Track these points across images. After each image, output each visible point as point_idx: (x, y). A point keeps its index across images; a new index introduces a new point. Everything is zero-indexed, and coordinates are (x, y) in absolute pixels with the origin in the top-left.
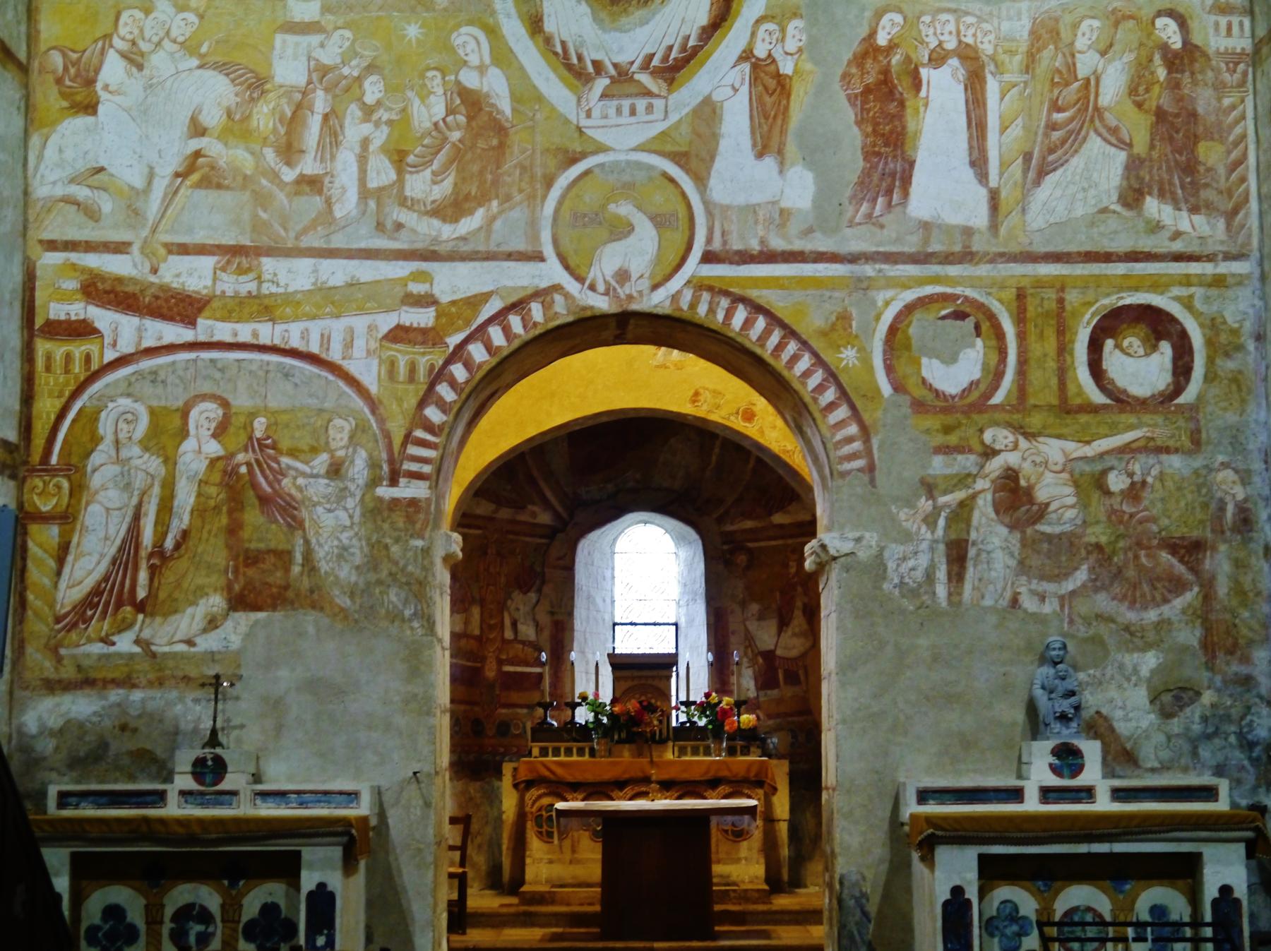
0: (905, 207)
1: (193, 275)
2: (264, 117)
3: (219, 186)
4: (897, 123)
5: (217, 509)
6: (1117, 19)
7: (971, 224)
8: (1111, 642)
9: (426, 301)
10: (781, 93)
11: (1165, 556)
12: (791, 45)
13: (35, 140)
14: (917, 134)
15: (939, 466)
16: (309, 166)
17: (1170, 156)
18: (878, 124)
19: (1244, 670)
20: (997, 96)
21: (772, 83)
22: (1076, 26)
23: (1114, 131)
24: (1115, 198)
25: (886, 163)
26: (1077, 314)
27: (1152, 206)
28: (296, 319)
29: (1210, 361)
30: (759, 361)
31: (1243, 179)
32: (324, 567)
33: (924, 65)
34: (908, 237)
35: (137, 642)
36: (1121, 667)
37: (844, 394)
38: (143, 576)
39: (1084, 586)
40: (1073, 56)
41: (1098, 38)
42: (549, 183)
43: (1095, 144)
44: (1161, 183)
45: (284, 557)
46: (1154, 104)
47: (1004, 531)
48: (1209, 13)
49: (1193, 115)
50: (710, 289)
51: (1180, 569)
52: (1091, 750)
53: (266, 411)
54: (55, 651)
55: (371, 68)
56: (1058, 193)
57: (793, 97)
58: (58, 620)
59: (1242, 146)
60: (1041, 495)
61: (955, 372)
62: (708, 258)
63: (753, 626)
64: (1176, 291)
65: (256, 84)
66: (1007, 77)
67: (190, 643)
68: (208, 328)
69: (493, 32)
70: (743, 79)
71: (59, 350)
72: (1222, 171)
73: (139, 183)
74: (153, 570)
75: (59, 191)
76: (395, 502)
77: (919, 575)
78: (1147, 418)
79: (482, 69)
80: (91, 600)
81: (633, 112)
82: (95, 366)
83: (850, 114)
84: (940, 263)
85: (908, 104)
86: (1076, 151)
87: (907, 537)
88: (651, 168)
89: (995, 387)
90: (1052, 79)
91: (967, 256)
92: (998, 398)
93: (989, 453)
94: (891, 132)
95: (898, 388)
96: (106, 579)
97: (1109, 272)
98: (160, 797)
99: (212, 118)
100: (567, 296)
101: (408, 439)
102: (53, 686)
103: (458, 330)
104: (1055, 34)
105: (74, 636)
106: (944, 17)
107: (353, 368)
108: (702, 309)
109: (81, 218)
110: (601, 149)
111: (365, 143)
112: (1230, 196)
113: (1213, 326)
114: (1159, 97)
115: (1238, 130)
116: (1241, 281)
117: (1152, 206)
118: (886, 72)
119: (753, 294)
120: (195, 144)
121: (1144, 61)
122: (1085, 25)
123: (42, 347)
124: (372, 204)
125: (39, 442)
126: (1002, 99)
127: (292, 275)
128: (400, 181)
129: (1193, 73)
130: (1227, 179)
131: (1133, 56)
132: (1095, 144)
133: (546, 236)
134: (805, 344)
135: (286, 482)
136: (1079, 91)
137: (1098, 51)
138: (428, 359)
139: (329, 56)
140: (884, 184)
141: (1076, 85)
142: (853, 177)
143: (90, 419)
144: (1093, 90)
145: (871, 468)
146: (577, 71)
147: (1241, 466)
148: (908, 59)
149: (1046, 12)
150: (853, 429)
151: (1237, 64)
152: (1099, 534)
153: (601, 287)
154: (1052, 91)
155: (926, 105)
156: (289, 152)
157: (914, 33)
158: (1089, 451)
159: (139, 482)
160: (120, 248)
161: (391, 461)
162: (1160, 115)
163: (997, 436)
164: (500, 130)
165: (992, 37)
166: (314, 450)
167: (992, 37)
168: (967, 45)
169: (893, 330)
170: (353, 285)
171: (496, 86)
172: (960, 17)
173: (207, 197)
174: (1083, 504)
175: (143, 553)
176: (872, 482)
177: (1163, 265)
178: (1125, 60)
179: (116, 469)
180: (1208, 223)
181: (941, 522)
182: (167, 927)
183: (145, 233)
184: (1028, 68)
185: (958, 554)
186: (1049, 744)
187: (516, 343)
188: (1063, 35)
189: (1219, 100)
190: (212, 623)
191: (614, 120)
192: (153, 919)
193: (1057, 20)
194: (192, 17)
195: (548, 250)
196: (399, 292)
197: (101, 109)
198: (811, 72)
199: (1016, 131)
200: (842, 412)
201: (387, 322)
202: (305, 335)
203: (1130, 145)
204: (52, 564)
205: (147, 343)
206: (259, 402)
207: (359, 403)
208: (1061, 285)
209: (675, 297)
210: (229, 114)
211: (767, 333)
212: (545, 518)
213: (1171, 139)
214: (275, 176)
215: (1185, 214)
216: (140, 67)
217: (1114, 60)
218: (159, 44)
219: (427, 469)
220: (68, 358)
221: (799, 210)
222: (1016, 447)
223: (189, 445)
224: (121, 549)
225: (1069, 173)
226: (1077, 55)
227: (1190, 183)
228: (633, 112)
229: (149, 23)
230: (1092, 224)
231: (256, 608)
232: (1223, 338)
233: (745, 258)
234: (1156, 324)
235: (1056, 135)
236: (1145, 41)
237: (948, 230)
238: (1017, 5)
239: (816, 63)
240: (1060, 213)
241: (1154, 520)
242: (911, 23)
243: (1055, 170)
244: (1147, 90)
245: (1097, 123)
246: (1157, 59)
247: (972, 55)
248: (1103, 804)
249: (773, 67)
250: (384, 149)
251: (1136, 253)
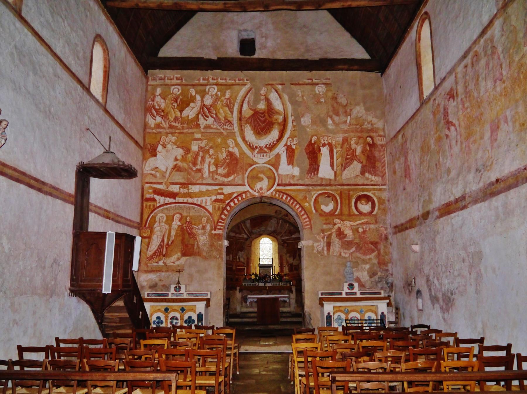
1: (175, 188)
2: (190, 157)
3: (181, 171)
5: (180, 236)
6: (359, 138)
8: (359, 262)
9: (222, 194)
11: (370, 245)
12: (295, 143)
13: (144, 162)
14: (320, 160)
15: (325, 227)
16: (198, 167)
19: (386, 268)
21: (291, 150)
22: (351, 139)
26: (352, 196)
28: (196, 197)
29: (379, 206)
30: (288, 205)
31: (385, 169)
32: (201, 247)
35: (163, 263)
36: (362, 268)
37: (305, 212)
38: (165, 250)
39: (354, 251)
42: (246, 170)
43: (355, 162)
45: (193, 245)
47: (338, 240)
50: (279, 191)
51: (373, 247)
52: (356, 285)
53: (189, 216)
54: (147, 264)
55: (211, 147)
58: (147, 258)
60: (346, 233)
61: (328, 208)
62: (278, 185)
63: (288, 259)
64: (372, 192)
65: (187, 150)
66: (338, 149)
67: (174, 263)
68: (178, 199)
69: (235, 140)
71: (148, 204)
73: (164, 170)
74: (166, 248)
75: (149, 172)
76: (215, 234)
77: (321, 249)
78: (367, 217)
79: (233, 148)
80: (154, 254)
81: (263, 156)
82: (155, 207)
83: (306, 156)
87: (318, 241)
88: (267, 167)
89: (336, 211)
91: (330, 185)
92: (336, 213)
93: (335, 224)
95: (316, 211)
96: (157, 250)
98: (168, 294)
99: (179, 157)
100: (250, 193)
101: (218, 222)
102: (147, 272)
103: (228, 200)
104: (347, 140)
105: (150, 261)
107: (207, 207)
108: (277, 195)
109: (153, 177)
110: (257, 163)
111: (210, 162)
113: (379, 199)
116: (385, 190)
118: (314, 148)
119: (287, 192)
120: (176, 163)
123: (145, 203)
124: (211, 175)
125: (144, 222)
127: (195, 189)
128: (217, 170)
132: (355, 162)
133: (246, 181)
134: (298, 203)
135: (193, 230)
138: (222, 205)
139: (203, 144)
143: (154, 217)
145: (311, 228)
146: (252, 148)
147: (385, 227)
150: (307, 220)
152: (357, 241)
153: (257, 191)
156: (195, 164)
158: (355, 224)
159: (164, 230)
160: (161, 183)
161: (215, 226)
163: (336, 221)
164: (236, 159)
166: (199, 224)
169: (315, 200)
170: (207, 191)
171: (236, 151)
173: (179, 173)
174: (354, 234)
175: (165, 245)
176: (311, 230)
179: (158, 228)
181: (325, 238)
182: (169, 321)
183: (166, 180)
184: (342, 147)
185: (329, 244)
186: (347, 284)
187: (240, 202)
190: (178, 259)
191: (259, 158)
192: (166, 319)
194: (176, 138)
195: (246, 184)
196: (216, 192)
197: (157, 156)
199: (340, 160)
200: (305, 216)
201: (214, 198)
202: (197, 201)
204: (146, 247)
205: (166, 202)
206: (188, 214)
207: (208, 214)
208: (349, 190)
209: (272, 193)
210: (183, 156)
211: (290, 200)
212: (245, 236)
214: (191, 169)
216: (165, 147)
218: (169, 143)
219: (222, 228)
220: (150, 205)
222: (340, 223)
223: (174, 223)
224: (160, 244)
228: (263, 156)
229: (167, 139)
230: (355, 178)
231: (188, 256)
232: (381, 201)
233: (286, 185)
234: (368, 198)
235: (348, 160)
237: (326, 179)
240: (349, 176)
241: (368, 238)
242: (319, 139)
246: (367, 146)
248: (358, 295)
250: (213, 163)
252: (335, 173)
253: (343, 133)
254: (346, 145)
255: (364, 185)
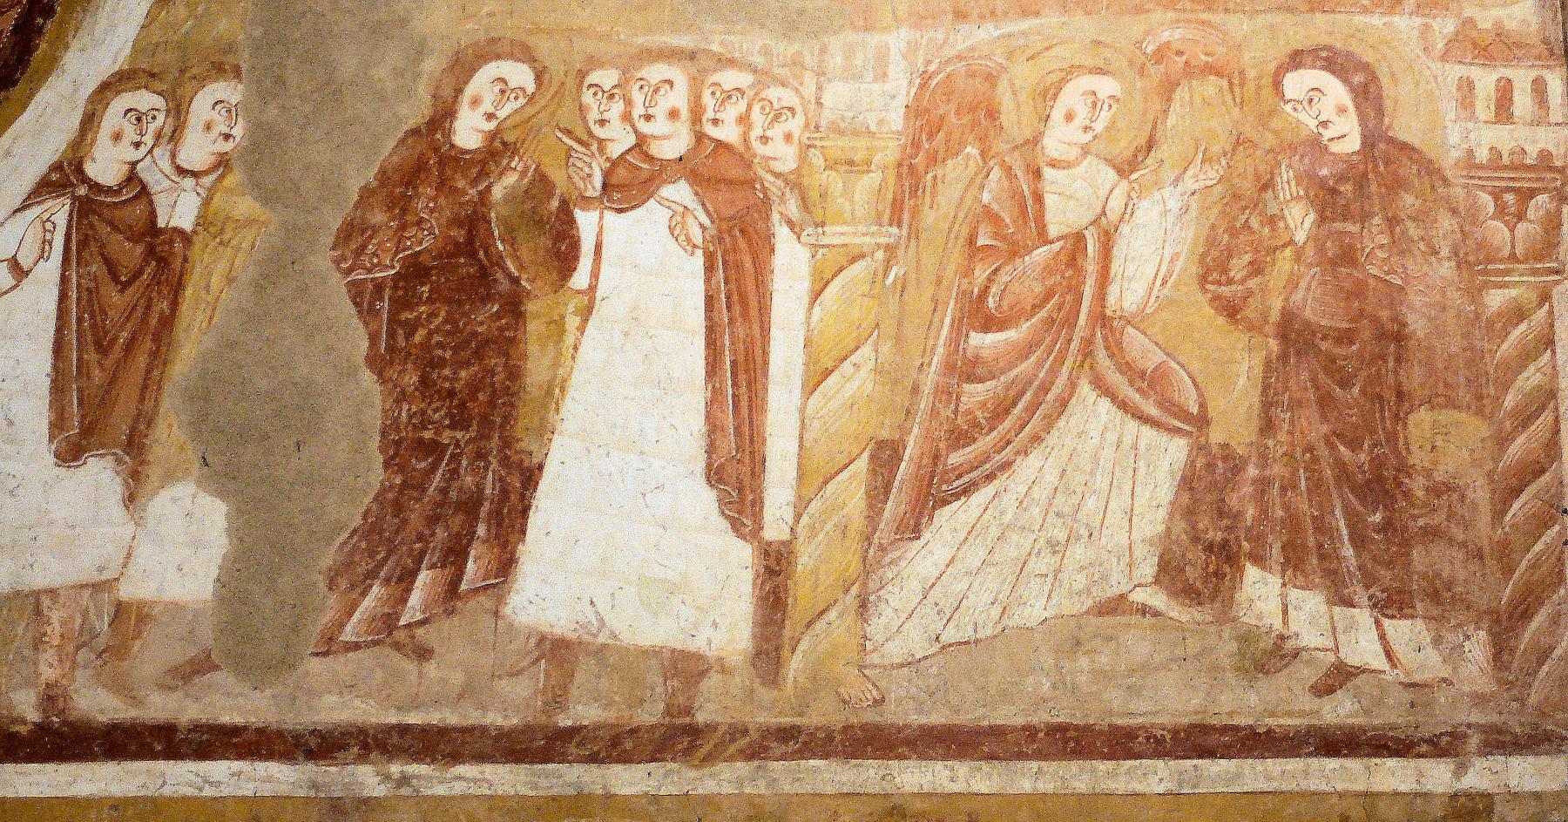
0: (501, 600)
4: (495, 361)
6: (1167, 76)
7: (698, 645)
10: (156, 280)
12: (197, 150)
14: (554, 391)
17: (1323, 451)
18: (442, 363)
20: (803, 287)
21: (130, 253)
22: (1048, 94)
23: (1152, 382)
24: (1148, 570)
25: (454, 473)
27: (1262, 593)
33: (586, 202)
34: (504, 685)
40: (1037, 174)
41: (1111, 126)
43: (1092, 419)
44: (1292, 522)
46: (1277, 304)
48: (1444, 57)
49: (1397, 336)
56: (974, 555)
57: (189, 292)
59: (1546, 418)
66: (834, 234)
70: (47, 243)
72: (1481, 494)
84: (593, 759)
85: (531, 307)
86: (1036, 439)
90: (971, 241)
91: (680, 739)
94: (474, 387)
97: (1120, 786)
104: (985, 116)
106: (656, 72)
112: (1505, 555)
114: (1294, 285)
115: (1531, 378)
117: (1262, 593)
118: (474, 221)
121: (1247, 186)
122: (1073, 96)
126: (816, 295)
129: (1392, 222)
130: (1499, 515)
131: (1212, 174)
132: (1092, 419)
136: (1048, 270)
137: (1109, 162)
140: (441, 533)
141: (1041, 254)
142: (348, 511)
144: (1091, 267)
148: (541, 183)
149: (960, 58)
151: (1527, 195)
154: (968, 272)
155: (587, 312)
157: (566, 116)
162: (1294, 336)
165: (795, 125)
167: (795, 125)
168: (720, 144)
172: (704, 72)
177: (1293, 764)
178: (1189, 183)
180: (1437, 641)
188: (1006, 119)
189: (1474, 294)
193: (991, 79)
198: (250, 222)
199: (855, 381)
203: (1202, 421)
213: (1325, 402)
215: (1363, 616)
217: (1158, 184)
221: (176, 608)
225: (1009, 501)
226: (1048, 172)
227: (1386, 527)
235: (976, 394)
236: (1249, 131)
238: (874, 39)
239: (268, 199)
240: (979, 614)
242: (558, 87)
243: (966, 491)
244: (1256, 269)
245: (1101, 356)
246: (1286, 179)
247: (736, 173)
249: (139, 209)
251: (1204, 729)
252: (775, 567)
253: (920, 20)
254: (958, 182)
255: (1198, 741)
